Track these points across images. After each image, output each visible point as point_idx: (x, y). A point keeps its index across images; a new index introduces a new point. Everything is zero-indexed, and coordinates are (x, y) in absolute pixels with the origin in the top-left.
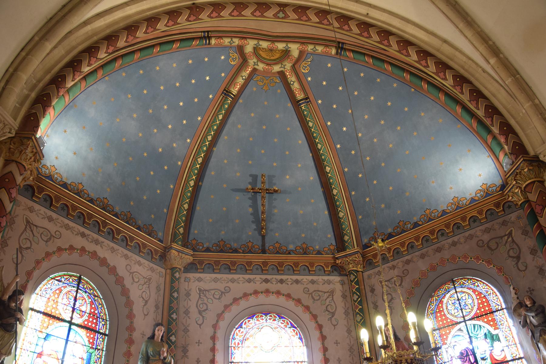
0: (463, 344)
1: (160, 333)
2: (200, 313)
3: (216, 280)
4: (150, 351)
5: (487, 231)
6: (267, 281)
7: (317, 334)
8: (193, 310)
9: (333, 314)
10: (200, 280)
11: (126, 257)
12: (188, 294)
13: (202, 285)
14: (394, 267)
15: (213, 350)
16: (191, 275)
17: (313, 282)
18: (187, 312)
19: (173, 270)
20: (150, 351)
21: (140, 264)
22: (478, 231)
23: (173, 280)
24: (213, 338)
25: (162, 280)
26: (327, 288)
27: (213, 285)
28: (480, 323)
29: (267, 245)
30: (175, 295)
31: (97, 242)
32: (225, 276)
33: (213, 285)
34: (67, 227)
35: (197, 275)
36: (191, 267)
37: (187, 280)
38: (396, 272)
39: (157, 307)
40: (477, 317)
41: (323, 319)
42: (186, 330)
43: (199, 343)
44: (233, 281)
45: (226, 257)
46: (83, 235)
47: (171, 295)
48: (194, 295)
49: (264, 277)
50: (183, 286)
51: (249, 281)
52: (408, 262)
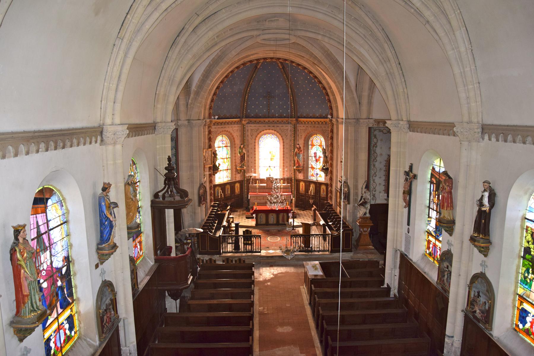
0: (315, 151)
1: (242, 146)
2: (251, 136)
3: (255, 126)
4: (240, 151)
5: (325, 127)
6: (269, 126)
7: (282, 141)
8: (250, 135)
9: (287, 136)
10: (251, 126)
11: (232, 127)
12: (248, 131)
13: (251, 128)
14: (304, 126)
15: (255, 146)
16: (248, 125)
17: (282, 126)
18: (248, 136)
19: (244, 125)
20: (240, 151)
21: (235, 127)
22: (323, 126)
23: (244, 128)
24: (255, 142)
25: (241, 128)
26: (287, 128)
27: (254, 128)
28: (319, 147)
29: (270, 115)
30: (245, 132)
31: (225, 127)
32: (258, 125)
33: (254, 128)
34: (219, 128)
35: (250, 125)
36: (248, 123)
37: (247, 126)
38: (304, 128)
39: (240, 136)
40: (319, 146)
41: (284, 137)
42: (248, 141)
43: (251, 144)
44: (260, 126)
45: (258, 120)
46: (222, 128)
47: (243, 132)
48: (250, 131)
49: (268, 125)
50: (247, 128)
51: (264, 126)
52: (307, 127)
